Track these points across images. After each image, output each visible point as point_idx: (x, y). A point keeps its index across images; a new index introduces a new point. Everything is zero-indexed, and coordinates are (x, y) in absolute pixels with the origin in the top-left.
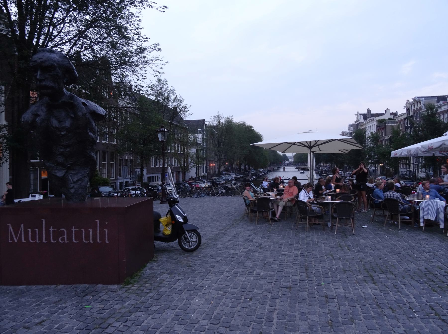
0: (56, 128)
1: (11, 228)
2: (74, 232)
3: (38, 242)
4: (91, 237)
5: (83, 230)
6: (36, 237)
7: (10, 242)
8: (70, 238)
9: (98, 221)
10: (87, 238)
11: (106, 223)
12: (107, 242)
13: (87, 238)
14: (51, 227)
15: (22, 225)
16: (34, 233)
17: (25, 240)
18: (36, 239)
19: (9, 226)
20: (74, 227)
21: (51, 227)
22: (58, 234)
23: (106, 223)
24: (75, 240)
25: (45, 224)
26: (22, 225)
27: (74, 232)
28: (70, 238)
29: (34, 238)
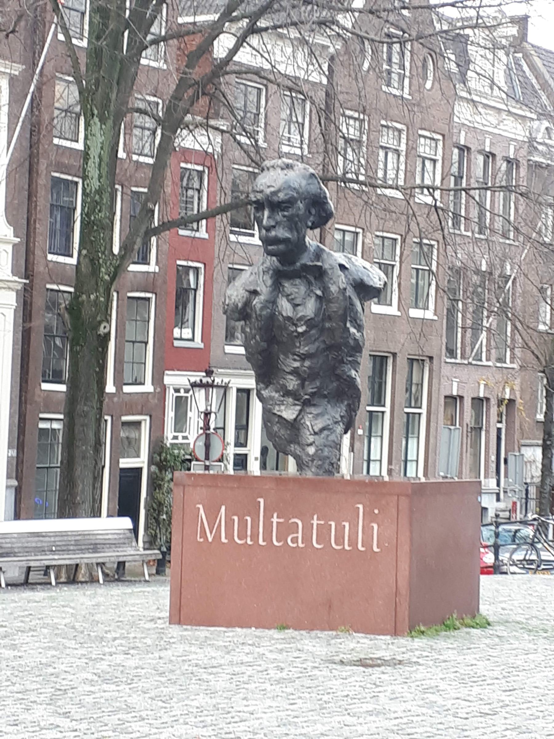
0: (289, 319)
1: (202, 511)
3: (249, 542)
5: (333, 524)
8: (307, 539)
10: (339, 539)
13: (339, 539)
14: (275, 515)
16: (243, 524)
20: (315, 517)
21: (275, 515)
24: (317, 543)
28: (307, 539)
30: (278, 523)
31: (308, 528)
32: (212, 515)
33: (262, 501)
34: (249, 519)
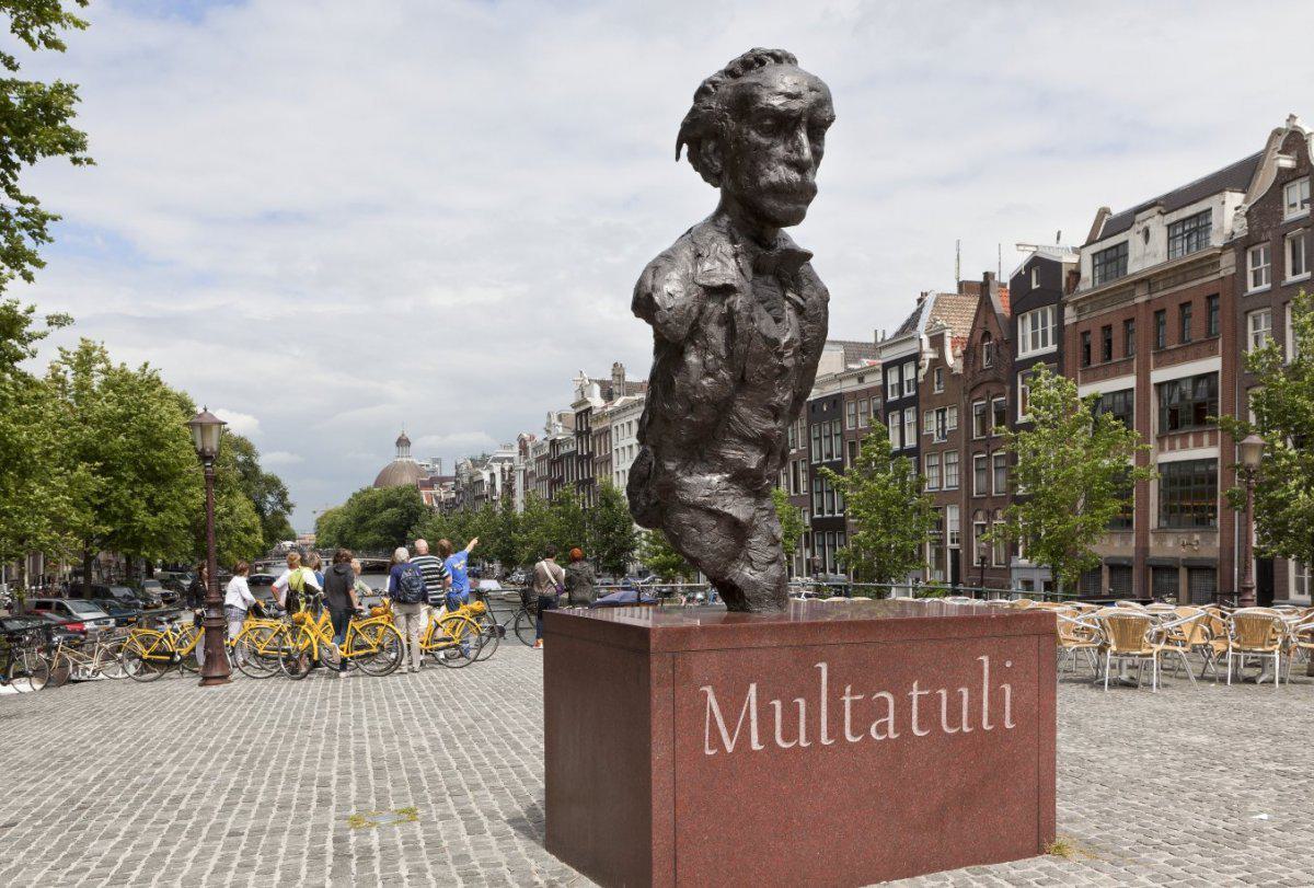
1: (712, 699)
2: (915, 702)
3: (803, 744)
4: (965, 713)
5: (943, 692)
6: (797, 728)
7: (709, 752)
8: (903, 723)
9: (985, 659)
10: (954, 718)
11: (1008, 664)
12: (1009, 725)
13: (954, 718)
15: (753, 687)
16: (791, 714)
17: (760, 743)
20: (915, 685)
24: (921, 728)
25: (830, 679)
26: (753, 687)
27: (915, 702)
30: (854, 703)
33: (824, 666)
34: (801, 702)
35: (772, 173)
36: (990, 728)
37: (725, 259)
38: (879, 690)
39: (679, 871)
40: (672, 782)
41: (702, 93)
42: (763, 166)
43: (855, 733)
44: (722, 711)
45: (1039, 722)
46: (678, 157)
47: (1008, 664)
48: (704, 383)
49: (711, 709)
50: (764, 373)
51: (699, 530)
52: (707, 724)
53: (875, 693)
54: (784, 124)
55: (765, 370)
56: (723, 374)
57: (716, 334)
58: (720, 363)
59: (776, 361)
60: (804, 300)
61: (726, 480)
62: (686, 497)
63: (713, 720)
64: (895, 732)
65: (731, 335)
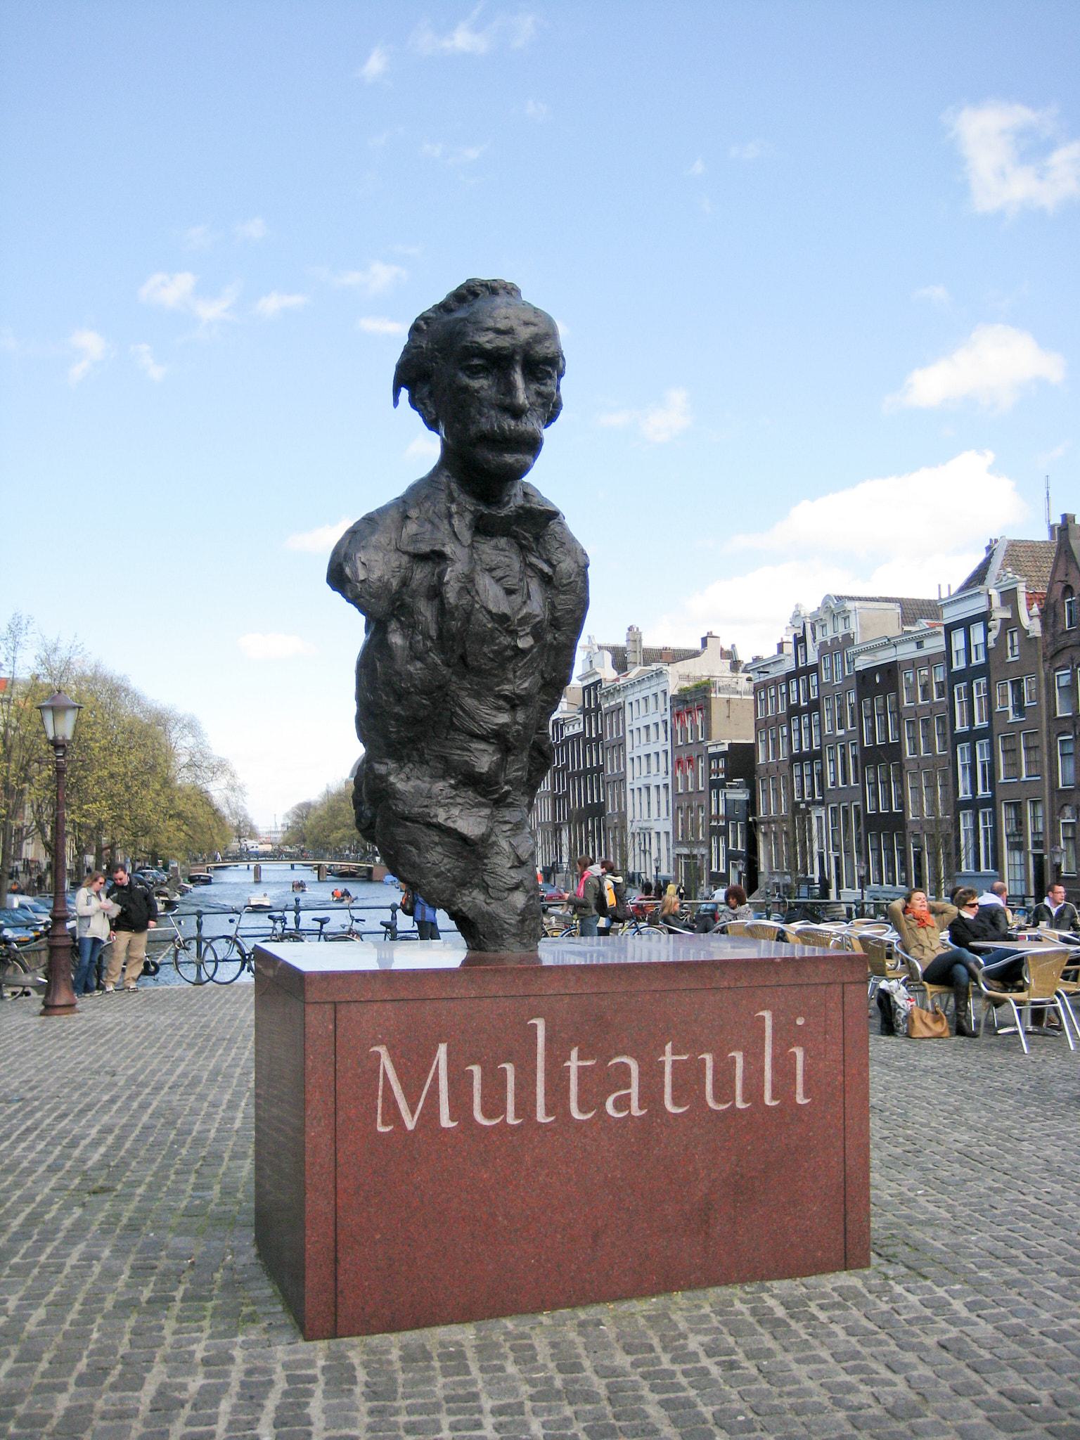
1: (386, 1063)
2: (668, 1069)
5: (708, 1058)
6: (504, 1100)
7: (381, 1129)
8: (651, 1096)
9: (767, 1015)
10: (724, 1092)
11: (800, 1022)
13: (724, 1092)
14: (574, 1053)
15: (442, 1049)
16: (494, 1084)
17: (452, 1119)
18: (504, 1111)
19: (378, 1056)
20: (668, 1047)
21: (574, 1053)
22: (599, 1083)
23: (800, 1022)
24: (676, 1102)
25: (549, 1039)
26: (442, 1049)
27: (668, 1069)
29: (494, 1106)
30: (581, 1070)
31: (651, 1075)
32: (414, 1070)
33: (540, 1024)
34: (509, 1068)
35: (483, 420)
36: (774, 1103)
37: (436, 520)
38: (617, 1054)
39: (340, 1278)
40: (333, 1164)
41: (415, 329)
42: (473, 411)
43: (583, 1108)
44: (400, 1077)
45: (845, 1094)
46: (396, 402)
47: (800, 1021)
48: (411, 668)
49: (385, 1074)
50: (491, 656)
51: (418, 848)
52: (380, 1093)
53: (611, 1058)
54: (498, 362)
55: (493, 652)
56: (435, 658)
57: (426, 611)
58: (429, 644)
59: (505, 640)
60: (552, 566)
61: (452, 786)
62: (401, 807)
63: (388, 1088)
64: (641, 1108)
65: (443, 612)
